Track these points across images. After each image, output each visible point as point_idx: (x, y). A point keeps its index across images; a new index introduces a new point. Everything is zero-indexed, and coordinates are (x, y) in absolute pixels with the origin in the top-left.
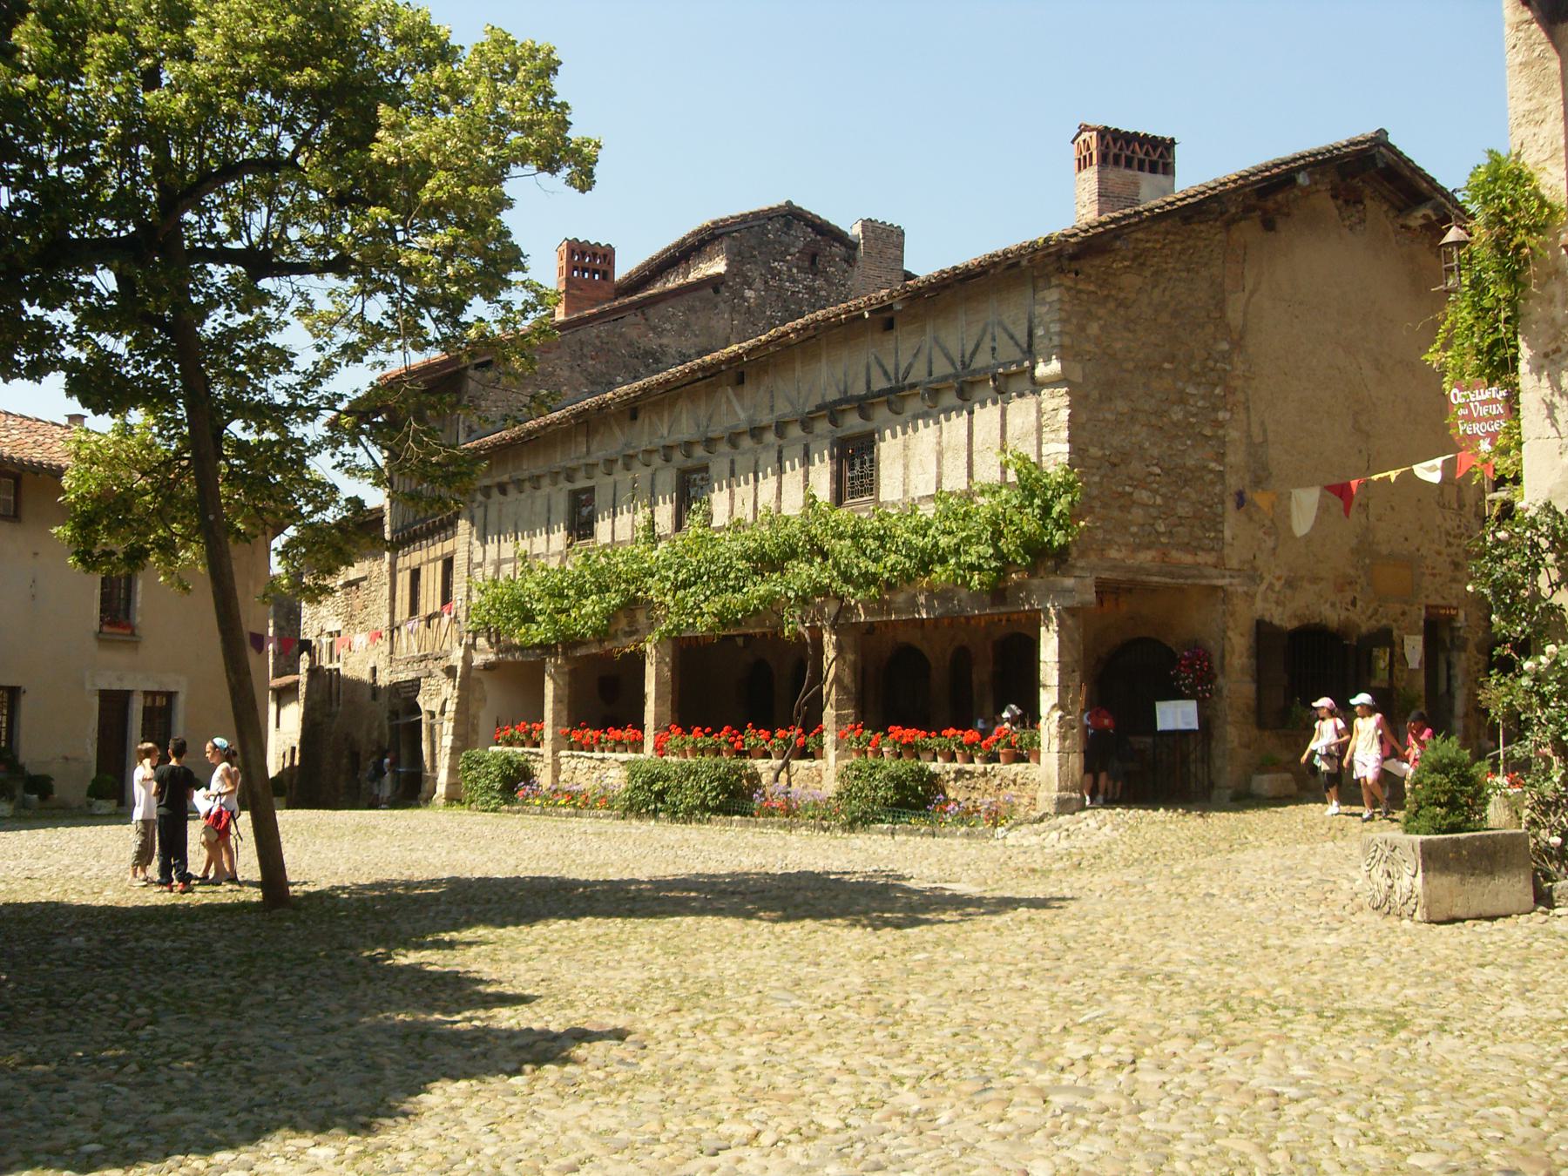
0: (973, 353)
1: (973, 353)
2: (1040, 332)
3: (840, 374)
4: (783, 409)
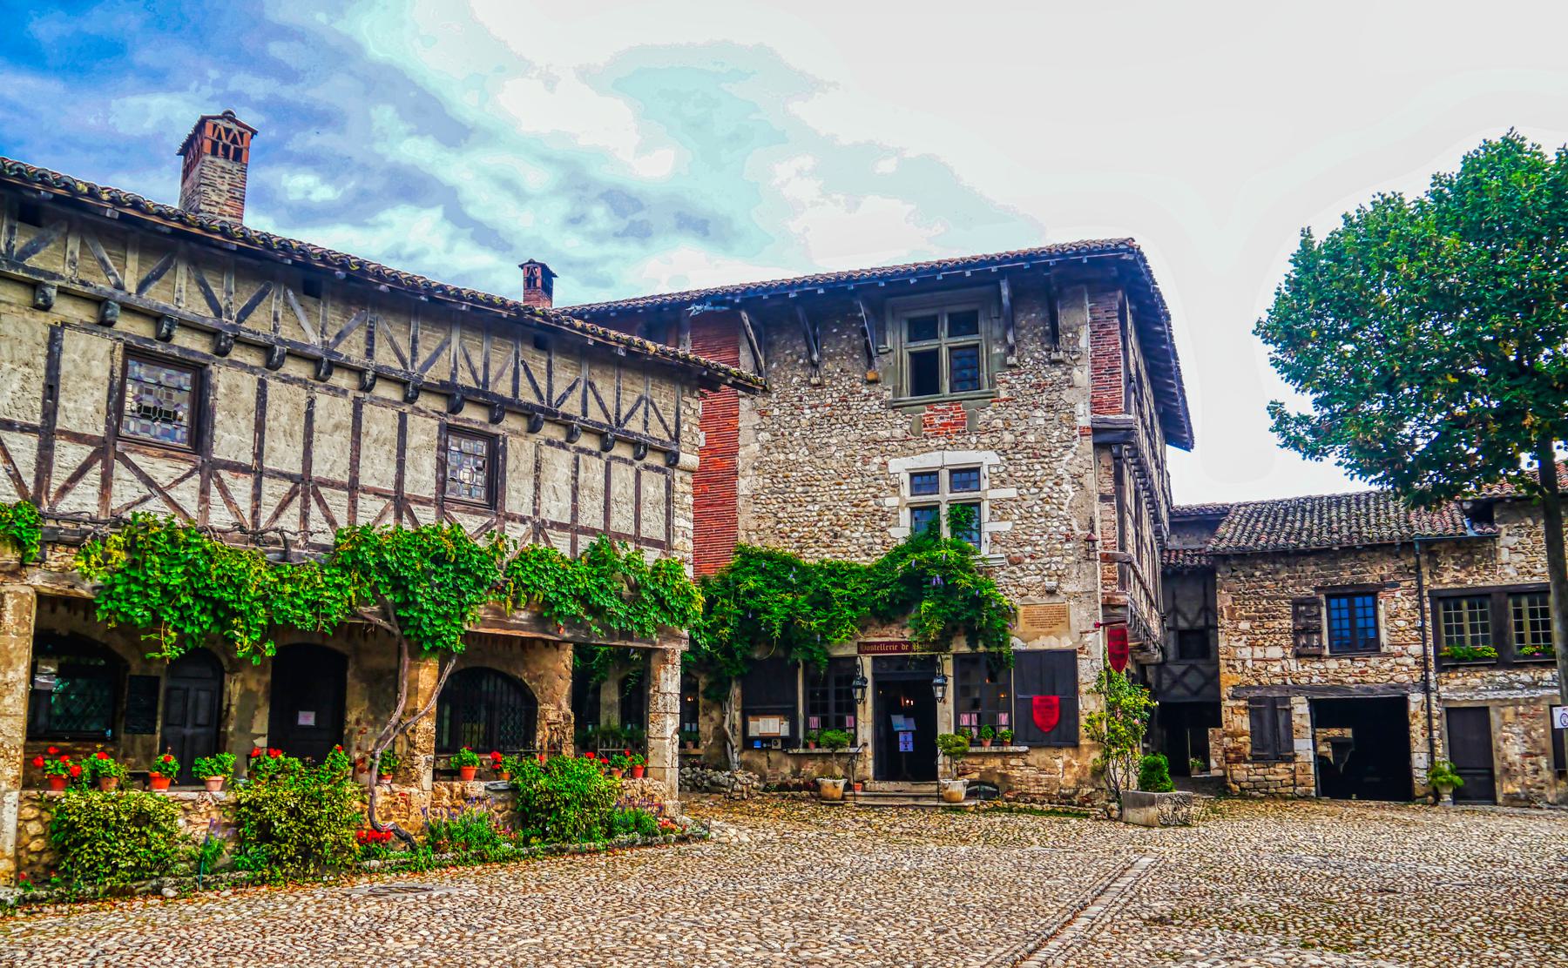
0: (628, 417)
1: (628, 417)
2: (686, 428)
3: (478, 362)
4: (384, 356)
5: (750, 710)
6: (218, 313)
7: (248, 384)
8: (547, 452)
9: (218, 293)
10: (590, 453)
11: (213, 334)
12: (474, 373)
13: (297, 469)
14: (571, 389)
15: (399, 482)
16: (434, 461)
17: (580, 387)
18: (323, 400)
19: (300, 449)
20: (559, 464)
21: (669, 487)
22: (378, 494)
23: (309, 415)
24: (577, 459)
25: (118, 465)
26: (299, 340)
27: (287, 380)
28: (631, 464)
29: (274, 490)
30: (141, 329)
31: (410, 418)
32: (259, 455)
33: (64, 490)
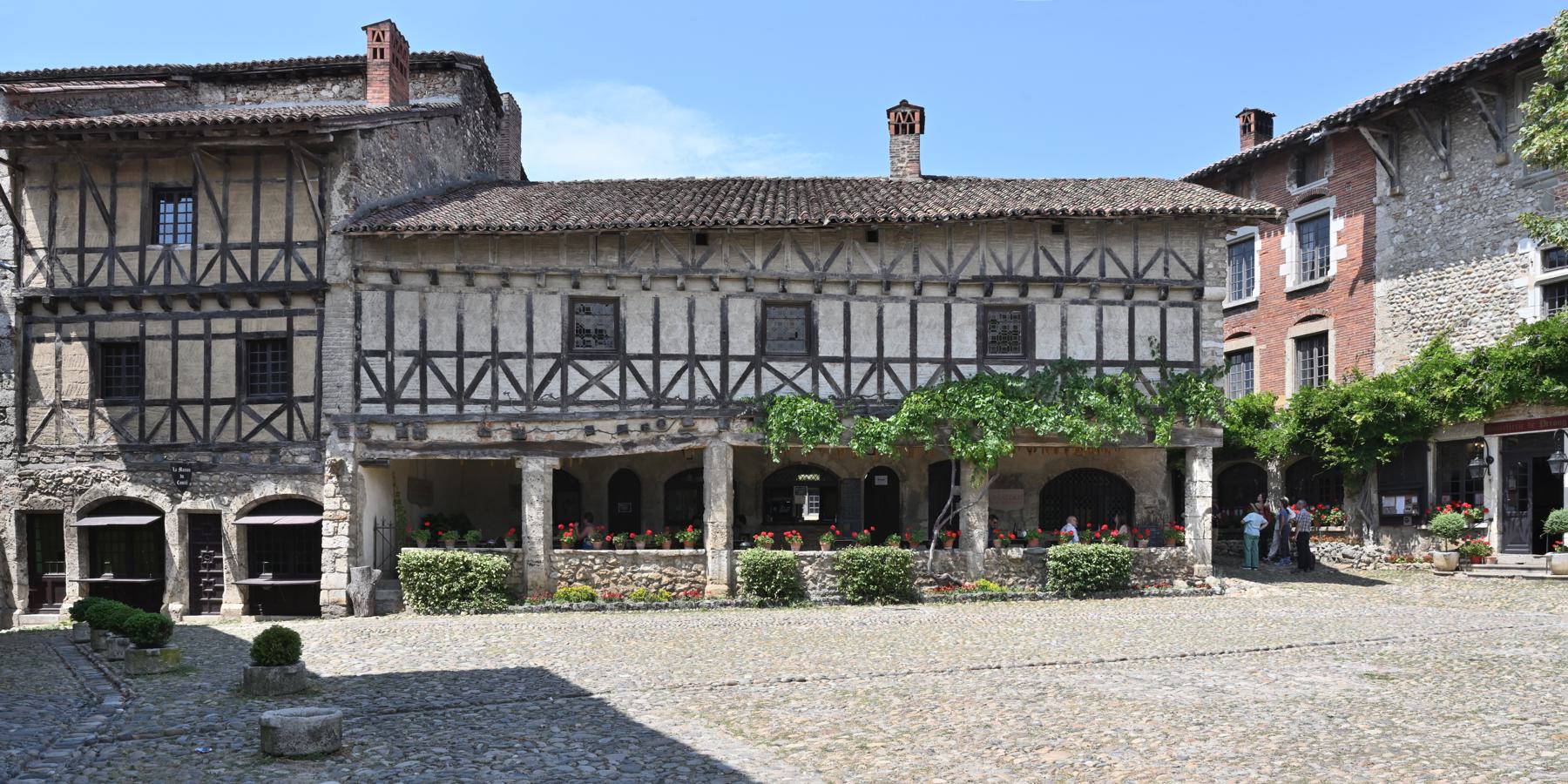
2: (1210, 266)
3: (1002, 255)
4: (927, 268)
5: (1384, 491)
6: (811, 268)
7: (838, 307)
8: (1072, 309)
9: (811, 256)
10: (1113, 303)
11: (812, 281)
12: (999, 265)
13: (874, 354)
14: (1088, 258)
15: (948, 349)
16: (974, 333)
17: (1097, 256)
18: (889, 308)
19: (875, 341)
20: (1084, 318)
21: (1197, 317)
22: (931, 361)
23: (880, 319)
24: (1100, 311)
25: (764, 370)
26: (865, 272)
27: (863, 299)
28: (1155, 304)
29: (858, 371)
30: (771, 288)
31: (954, 307)
32: (847, 348)
33: (736, 388)
